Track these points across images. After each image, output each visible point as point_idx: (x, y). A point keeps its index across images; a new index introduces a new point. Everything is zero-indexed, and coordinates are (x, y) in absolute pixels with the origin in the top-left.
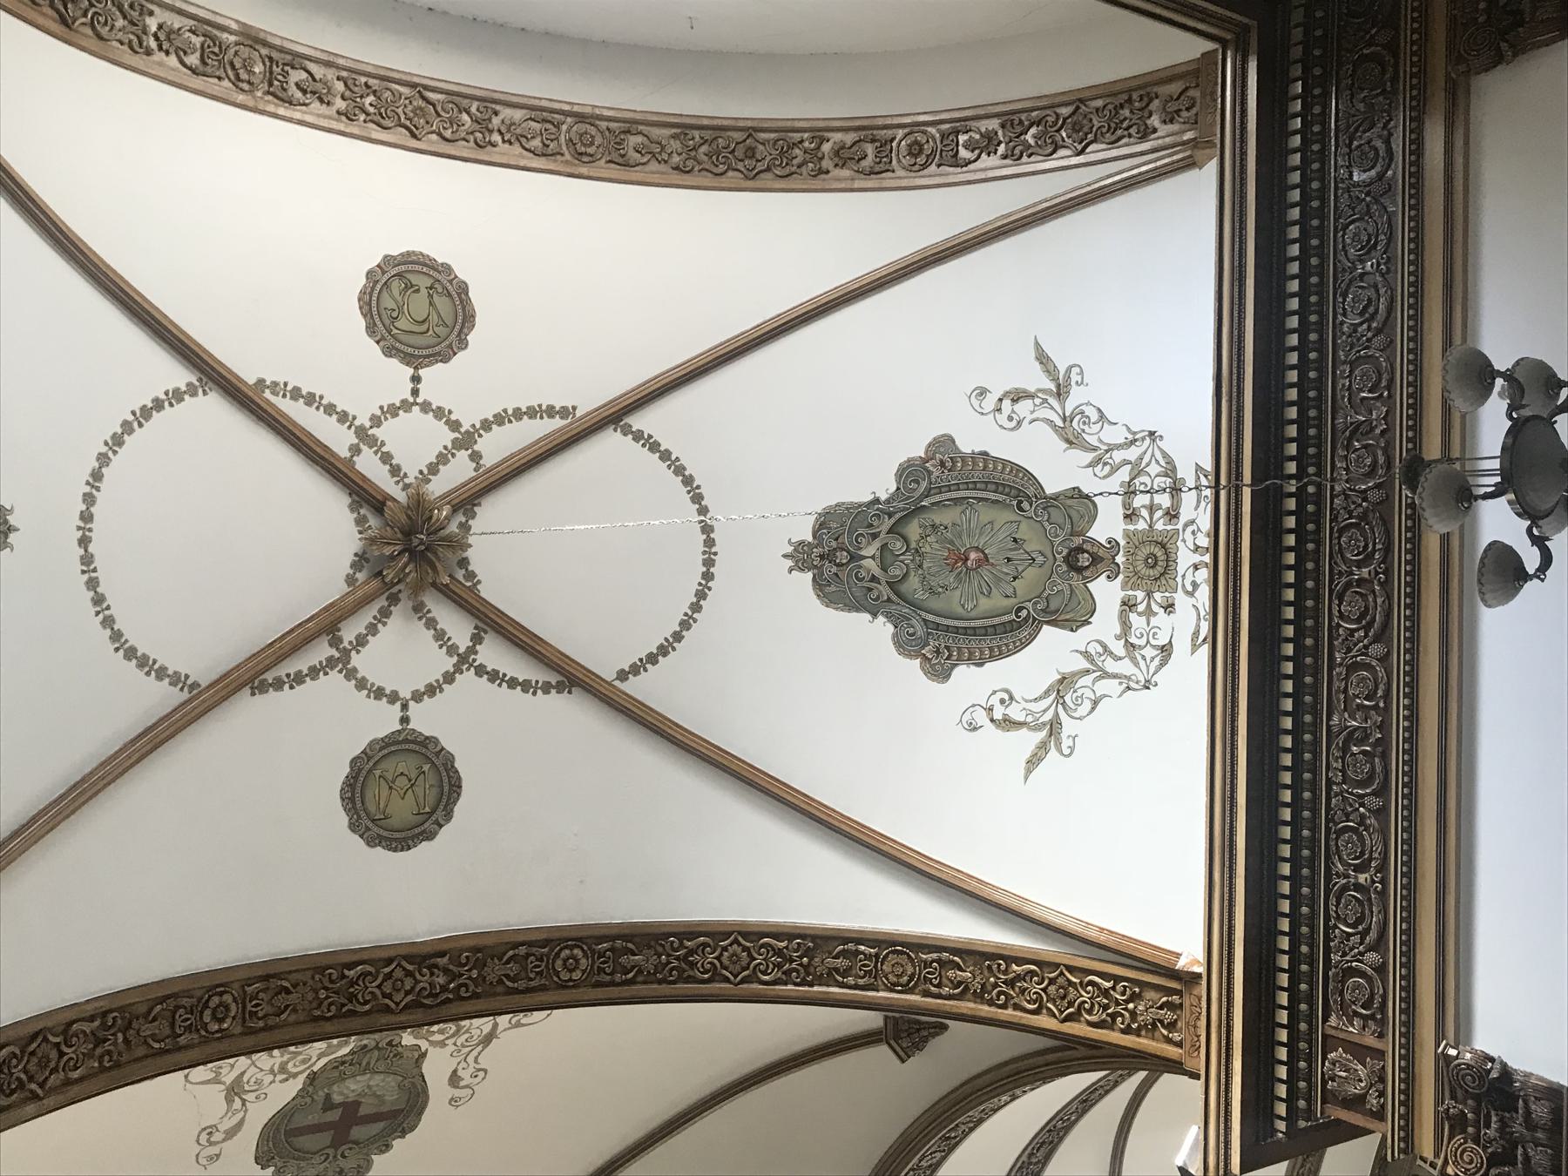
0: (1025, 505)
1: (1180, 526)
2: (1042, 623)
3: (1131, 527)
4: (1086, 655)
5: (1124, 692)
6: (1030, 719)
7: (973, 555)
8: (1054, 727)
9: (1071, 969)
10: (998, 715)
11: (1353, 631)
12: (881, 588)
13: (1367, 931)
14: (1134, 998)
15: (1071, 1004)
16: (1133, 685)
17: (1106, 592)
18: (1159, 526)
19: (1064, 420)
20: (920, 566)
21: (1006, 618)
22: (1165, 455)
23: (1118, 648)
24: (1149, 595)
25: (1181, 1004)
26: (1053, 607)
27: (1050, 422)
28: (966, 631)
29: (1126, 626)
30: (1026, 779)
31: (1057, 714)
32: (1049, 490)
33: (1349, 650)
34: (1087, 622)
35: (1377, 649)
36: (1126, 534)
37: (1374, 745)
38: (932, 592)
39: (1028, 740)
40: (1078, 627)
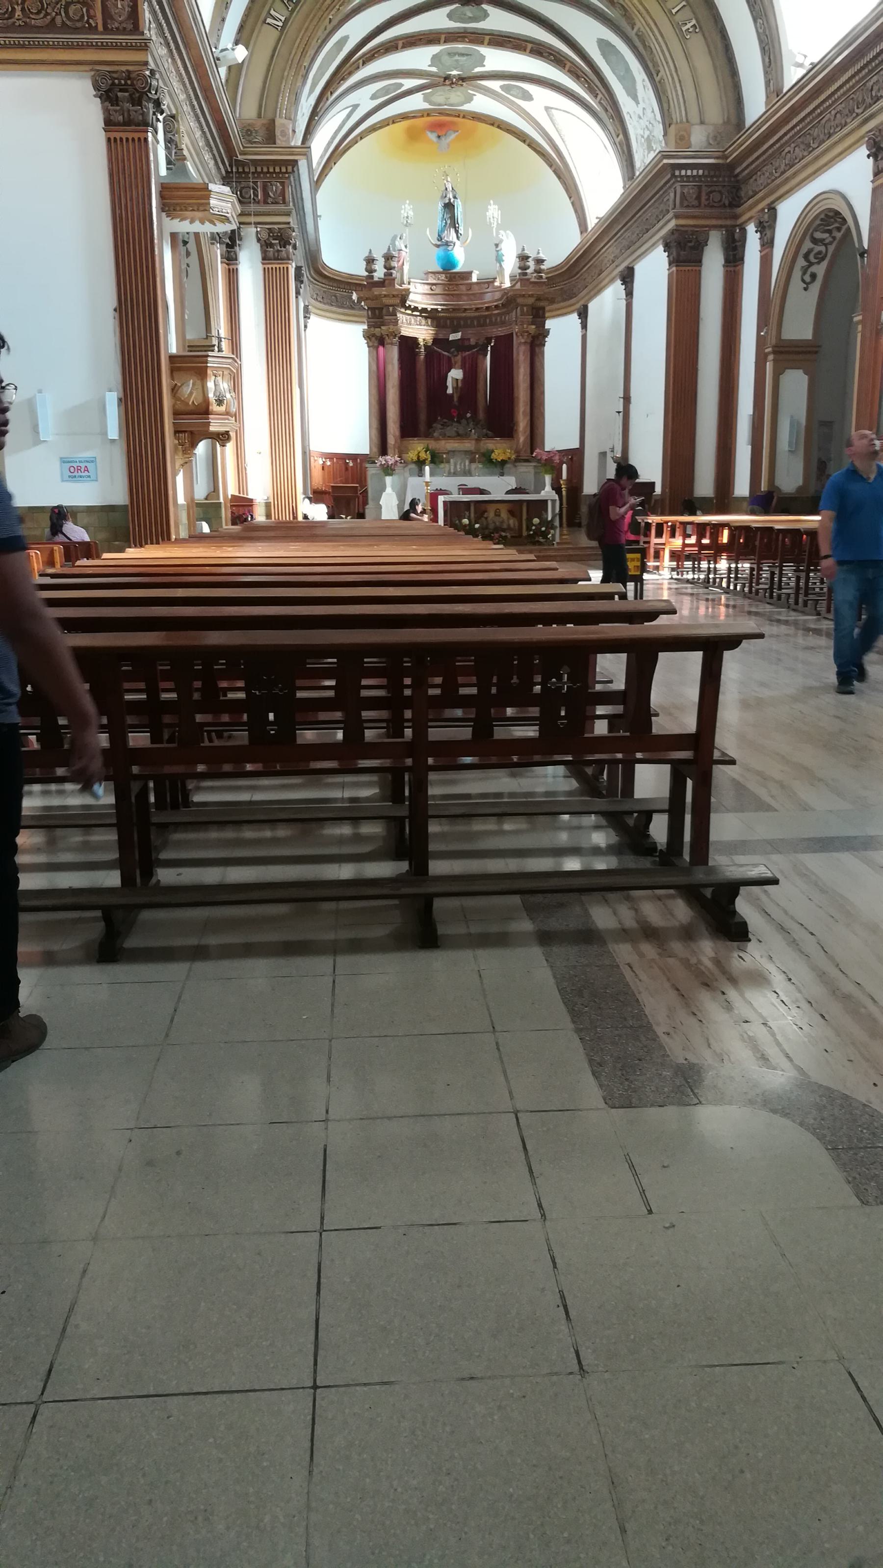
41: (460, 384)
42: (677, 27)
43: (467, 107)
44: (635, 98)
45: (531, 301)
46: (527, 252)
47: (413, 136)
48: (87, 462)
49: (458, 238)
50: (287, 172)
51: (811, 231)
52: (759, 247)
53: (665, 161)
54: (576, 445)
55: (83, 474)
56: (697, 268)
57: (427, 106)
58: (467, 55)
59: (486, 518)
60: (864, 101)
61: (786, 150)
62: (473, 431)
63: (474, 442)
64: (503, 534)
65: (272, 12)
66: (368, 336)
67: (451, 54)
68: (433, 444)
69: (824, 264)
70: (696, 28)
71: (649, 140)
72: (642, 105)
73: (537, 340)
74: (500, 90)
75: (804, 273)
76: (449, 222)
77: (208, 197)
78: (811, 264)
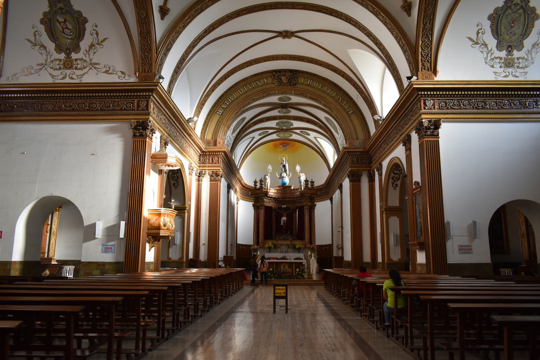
0: (522, 36)
1: (516, 69)
2: (498, 40)
3: (516, 59)
4: (491, 50)
5: (484, 58)
6: (479, 38)
7: (513, 25)
8: (477, 43)
9: (431, 48)
10: (480, 31)
11: (502, 103)
12: (510, 3)
13: (453, 106)
14: (428, 61)
15: (424, 48)
16: (486, 60)
17: (503, 54)
18: (516, 65)
19: (538, 44)
20: (513, 13)
21: (499, 32)
22: (529, 66)
23: (493, 57)
24: (503, 63)
25: (429, 71)
26: (501, 43)
27: (538, 41)
28: (498, 23)
29: (497, 58)
30: (467, 37)
31: (480, 44)
32: (524, 41)
33: (499, 102)
34: (497, 50)
35: (500, 107)
36: (514, 58)
37: (484, 107)
38: (507, 16)
39: (474, 38)
40: (496, 48)
41: (285, 222)
42: (347, 113)
43: (291, 138)
44: (337, 132)
45: (309, 195)
46: (308, 179)
47: (276, 146)
48: (112, 246)
49: (287, 175)
50: (219, 154)
51: (392, 170)
52: (378, 176)
53: (345, 150)
54: (330, 243)
55: (110, 250)
56: (359, 183)
57: (278, 138)
58: (287, 123)
59: (280, 269)
60: (400, 129)
61: (382, 146)
62: (290, 238)
63: (290, 241)
64: (286, 274)
65: (219, 110)
66: (254, 206)
67: (282, 123)
68: (275, 242)
69: (400, 181)
70: (353, 113)
71: (343, 145)
72: (340, 135)
73: (312, 208)
74: (299, 133)
75: (393, 184)
76: (284, 170)
77: (167, 158)
78: (395, 181)
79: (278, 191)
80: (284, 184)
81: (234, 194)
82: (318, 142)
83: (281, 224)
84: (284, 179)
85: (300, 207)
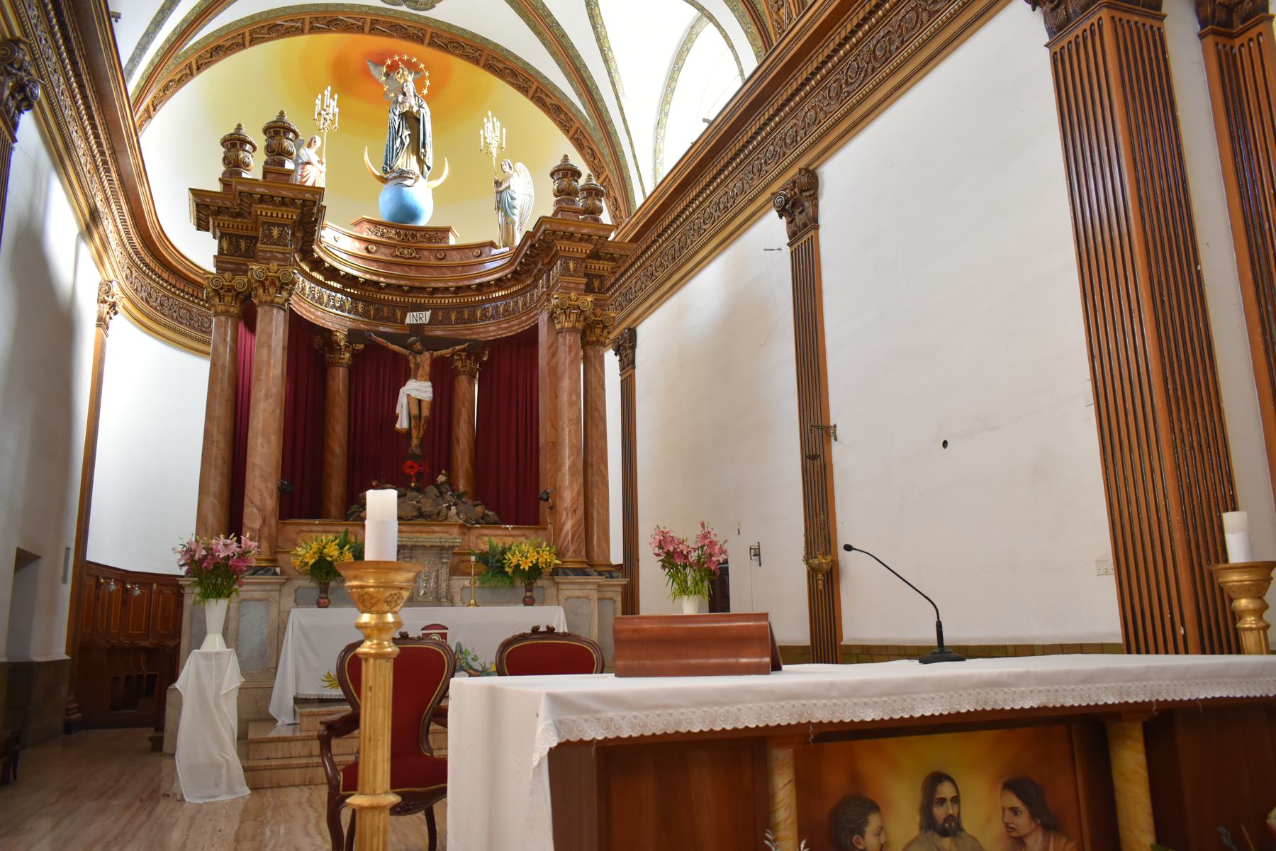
41: (426, 412)
62: (453, 508)
63: (456, 531)
76: (407, 142)
79: (373, 248)
80: (406, 213)
81: (81, 235)
82: (594, 27)
83: (398, 426)
84: (408, 182)
85: (497, 346)
